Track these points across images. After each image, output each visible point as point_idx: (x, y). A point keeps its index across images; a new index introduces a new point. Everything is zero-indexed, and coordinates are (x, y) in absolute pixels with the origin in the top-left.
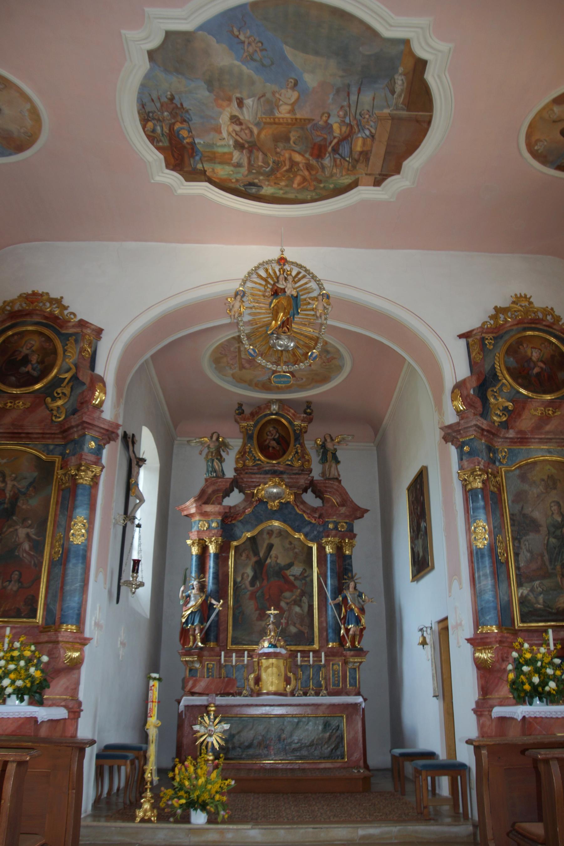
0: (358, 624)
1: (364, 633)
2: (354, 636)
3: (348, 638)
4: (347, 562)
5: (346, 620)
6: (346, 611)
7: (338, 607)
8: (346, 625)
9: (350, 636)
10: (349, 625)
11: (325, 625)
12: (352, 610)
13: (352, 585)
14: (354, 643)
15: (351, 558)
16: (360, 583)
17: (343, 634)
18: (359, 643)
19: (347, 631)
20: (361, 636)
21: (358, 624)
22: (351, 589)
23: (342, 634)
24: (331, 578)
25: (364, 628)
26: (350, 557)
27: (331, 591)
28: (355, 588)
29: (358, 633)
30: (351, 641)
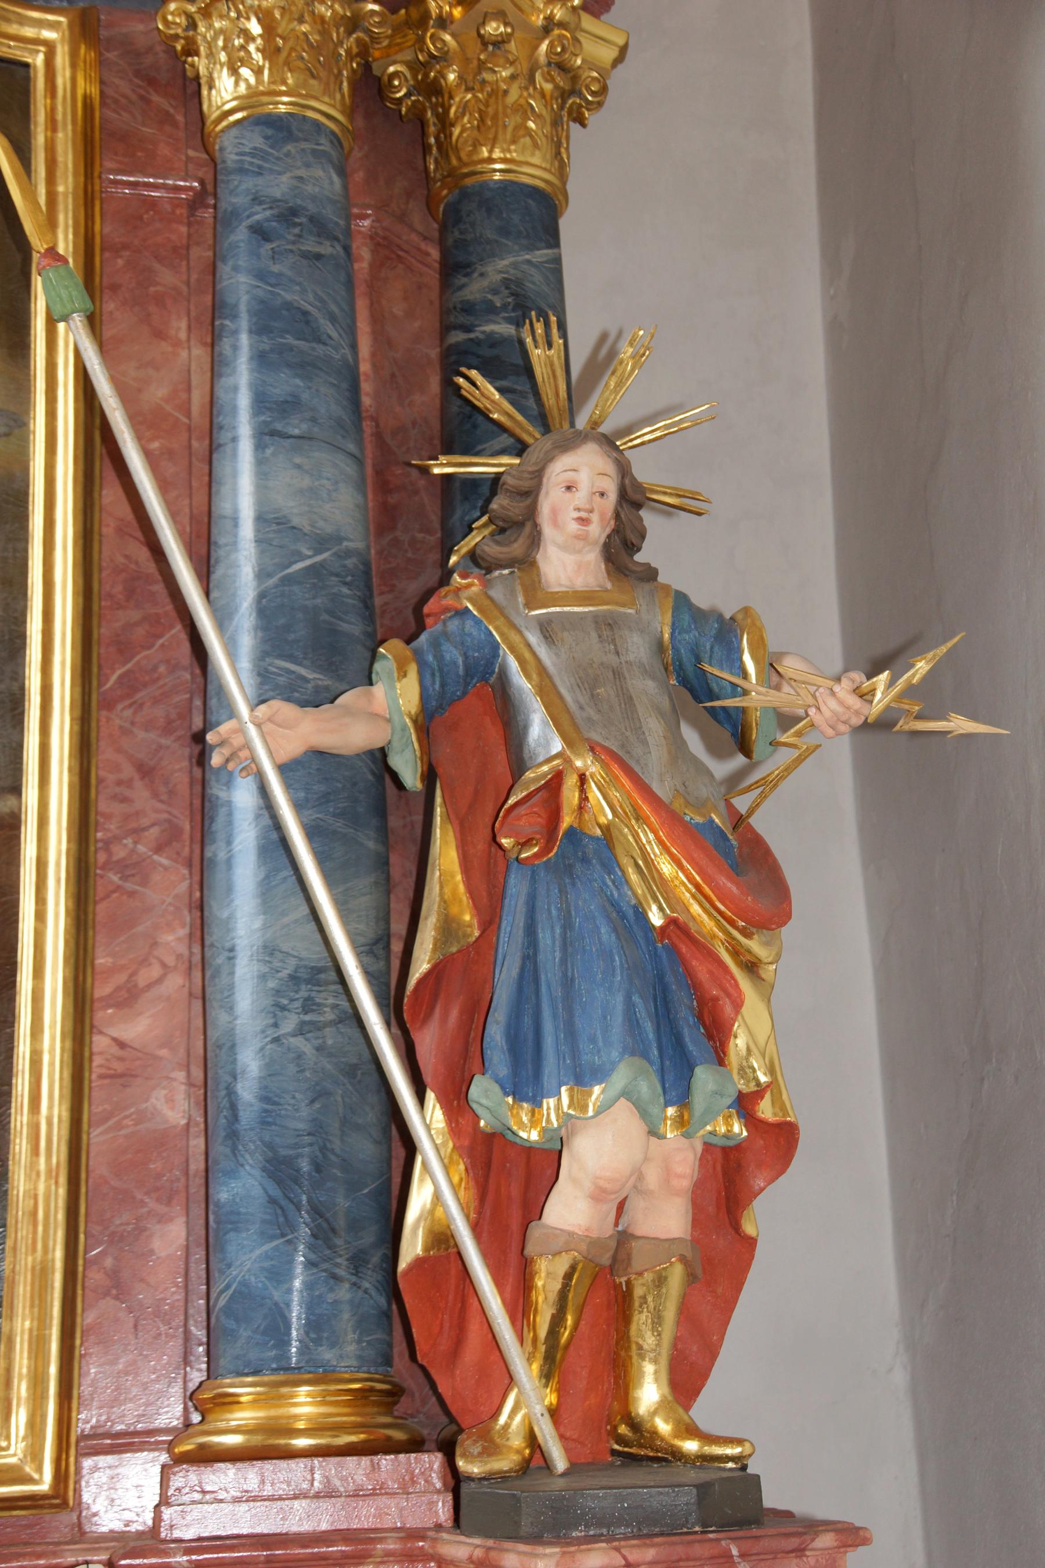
0: (677, 1086)
1: (767, 1215)
2: (607, 1284)
3: (520, 1308)
4: (497, 269)
5: (462, 1015)
6: (487, 875)
7: (371, 814)
8: (483, 1092)
9: (547, 1278)
10: (527, 1086)
11: (171, 1105)
12: (579, 854)
13: (574, 489)
14: (620, 1378)
15: (552, 237)
16: (687, 505)
17: (442, 1240)
18: (686, 1383)
19: (511, 1180)
20: (720, 1249)
21: (677, 1086)
22: (568, 558)
23: (413, 1246)
24: (266, 435)
25: (780, 1140)
26: (539, 214)
27: (266, 610)
28: (621, 548)
29: (667, 1219)
30: (553, 1364)
